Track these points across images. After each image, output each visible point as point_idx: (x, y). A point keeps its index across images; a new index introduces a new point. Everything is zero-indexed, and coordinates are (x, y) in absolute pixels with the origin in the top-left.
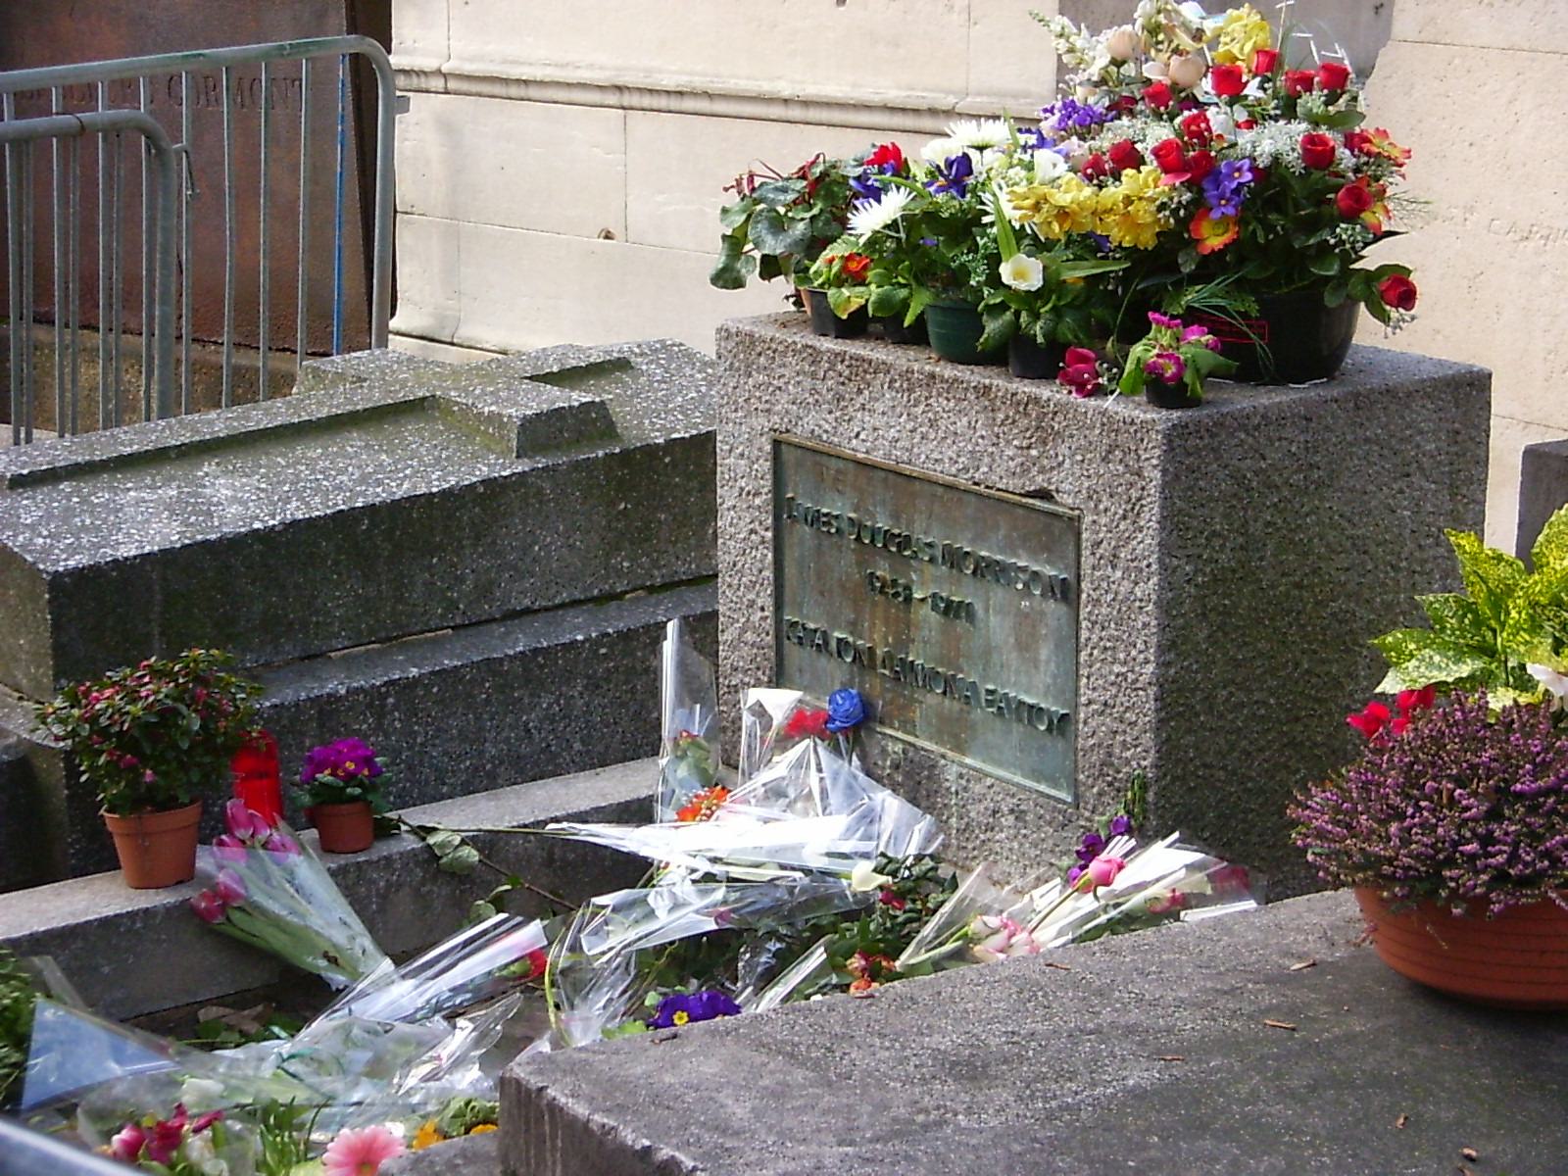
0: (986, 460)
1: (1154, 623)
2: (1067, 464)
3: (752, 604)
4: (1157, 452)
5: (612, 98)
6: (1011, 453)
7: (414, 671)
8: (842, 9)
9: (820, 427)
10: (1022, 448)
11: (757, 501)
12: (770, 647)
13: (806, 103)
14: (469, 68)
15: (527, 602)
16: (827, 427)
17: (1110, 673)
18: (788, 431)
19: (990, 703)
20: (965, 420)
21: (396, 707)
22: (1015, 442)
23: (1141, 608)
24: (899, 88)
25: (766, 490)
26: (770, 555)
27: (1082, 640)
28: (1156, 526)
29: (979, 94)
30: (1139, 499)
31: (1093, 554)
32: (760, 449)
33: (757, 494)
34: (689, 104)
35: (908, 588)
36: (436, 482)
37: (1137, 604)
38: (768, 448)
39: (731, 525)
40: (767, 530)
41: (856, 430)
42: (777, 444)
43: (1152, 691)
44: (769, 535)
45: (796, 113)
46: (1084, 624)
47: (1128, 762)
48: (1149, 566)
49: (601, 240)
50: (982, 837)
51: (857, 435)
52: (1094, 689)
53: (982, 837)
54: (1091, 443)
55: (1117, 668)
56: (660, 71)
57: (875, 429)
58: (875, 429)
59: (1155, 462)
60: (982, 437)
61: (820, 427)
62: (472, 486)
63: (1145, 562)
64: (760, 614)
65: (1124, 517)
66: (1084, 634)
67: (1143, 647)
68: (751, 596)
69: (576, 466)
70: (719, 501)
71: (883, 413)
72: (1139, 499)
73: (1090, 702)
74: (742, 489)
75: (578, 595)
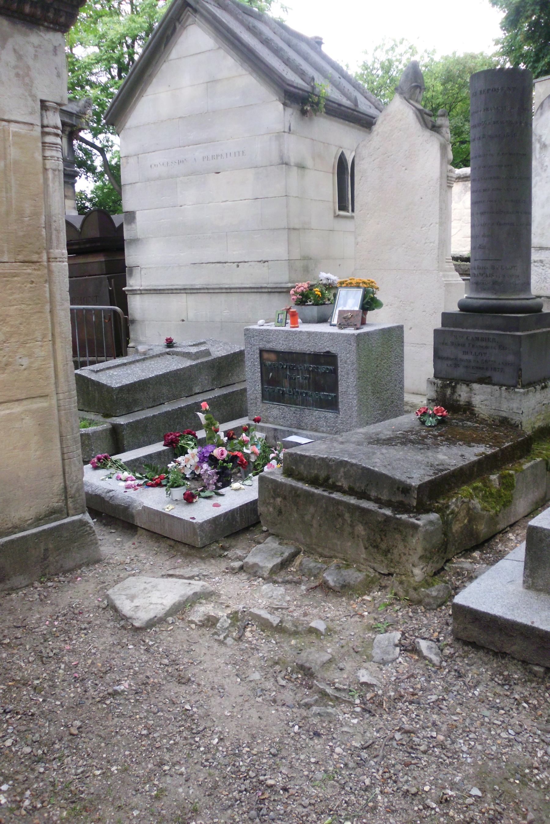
13: (231, 288)
14: (147, 288)
36: (181, 366)
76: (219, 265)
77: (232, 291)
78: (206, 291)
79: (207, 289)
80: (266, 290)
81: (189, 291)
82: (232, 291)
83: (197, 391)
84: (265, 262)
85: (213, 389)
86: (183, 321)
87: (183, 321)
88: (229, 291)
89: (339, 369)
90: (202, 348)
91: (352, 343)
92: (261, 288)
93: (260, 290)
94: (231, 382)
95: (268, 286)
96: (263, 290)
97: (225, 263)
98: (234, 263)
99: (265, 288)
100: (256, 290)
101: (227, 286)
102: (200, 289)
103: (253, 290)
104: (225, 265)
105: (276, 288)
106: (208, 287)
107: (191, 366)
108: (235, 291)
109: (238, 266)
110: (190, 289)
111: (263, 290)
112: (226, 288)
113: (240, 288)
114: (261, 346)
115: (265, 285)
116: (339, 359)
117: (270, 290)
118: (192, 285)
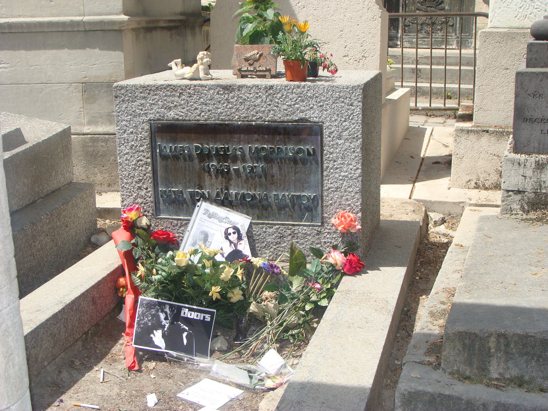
0: (272, 112)
1: (360, 155)
2: (315, 107)
3: (140, 188)
10: (290, 106)
11: (142, 148)
12: (152, 202)
17: (339, 176)
20: (260, 100)
22: (287, 104)
26: (150, 168)
27: (325, 167)
28: (360, 122)
30: (352, 114)
31: (330, 137)
33: (141, 146)
37: (352, 150)
38: (147, 127)
39: (126, 160)
40: (147, 158)
41: (199, 113)
43: (360, 179)
44: (149, 160)
46: (325, 162)
47: (349, 205)
48: (357, 136)
50: (275, 247)
51: (199, 115)
52: (331, 183)
54: (327, 98)
55: (343, 174)
57: (209, 111)
59: (359, 99)
65: (345, 121)
66: (325, 165)
68: (140, 184)
71: (214, 104)
72: (352, 114)
73: (329, 188)
74: (133, 145)
91: (356, 103)
114: (151, 116)
116: (326, 132)
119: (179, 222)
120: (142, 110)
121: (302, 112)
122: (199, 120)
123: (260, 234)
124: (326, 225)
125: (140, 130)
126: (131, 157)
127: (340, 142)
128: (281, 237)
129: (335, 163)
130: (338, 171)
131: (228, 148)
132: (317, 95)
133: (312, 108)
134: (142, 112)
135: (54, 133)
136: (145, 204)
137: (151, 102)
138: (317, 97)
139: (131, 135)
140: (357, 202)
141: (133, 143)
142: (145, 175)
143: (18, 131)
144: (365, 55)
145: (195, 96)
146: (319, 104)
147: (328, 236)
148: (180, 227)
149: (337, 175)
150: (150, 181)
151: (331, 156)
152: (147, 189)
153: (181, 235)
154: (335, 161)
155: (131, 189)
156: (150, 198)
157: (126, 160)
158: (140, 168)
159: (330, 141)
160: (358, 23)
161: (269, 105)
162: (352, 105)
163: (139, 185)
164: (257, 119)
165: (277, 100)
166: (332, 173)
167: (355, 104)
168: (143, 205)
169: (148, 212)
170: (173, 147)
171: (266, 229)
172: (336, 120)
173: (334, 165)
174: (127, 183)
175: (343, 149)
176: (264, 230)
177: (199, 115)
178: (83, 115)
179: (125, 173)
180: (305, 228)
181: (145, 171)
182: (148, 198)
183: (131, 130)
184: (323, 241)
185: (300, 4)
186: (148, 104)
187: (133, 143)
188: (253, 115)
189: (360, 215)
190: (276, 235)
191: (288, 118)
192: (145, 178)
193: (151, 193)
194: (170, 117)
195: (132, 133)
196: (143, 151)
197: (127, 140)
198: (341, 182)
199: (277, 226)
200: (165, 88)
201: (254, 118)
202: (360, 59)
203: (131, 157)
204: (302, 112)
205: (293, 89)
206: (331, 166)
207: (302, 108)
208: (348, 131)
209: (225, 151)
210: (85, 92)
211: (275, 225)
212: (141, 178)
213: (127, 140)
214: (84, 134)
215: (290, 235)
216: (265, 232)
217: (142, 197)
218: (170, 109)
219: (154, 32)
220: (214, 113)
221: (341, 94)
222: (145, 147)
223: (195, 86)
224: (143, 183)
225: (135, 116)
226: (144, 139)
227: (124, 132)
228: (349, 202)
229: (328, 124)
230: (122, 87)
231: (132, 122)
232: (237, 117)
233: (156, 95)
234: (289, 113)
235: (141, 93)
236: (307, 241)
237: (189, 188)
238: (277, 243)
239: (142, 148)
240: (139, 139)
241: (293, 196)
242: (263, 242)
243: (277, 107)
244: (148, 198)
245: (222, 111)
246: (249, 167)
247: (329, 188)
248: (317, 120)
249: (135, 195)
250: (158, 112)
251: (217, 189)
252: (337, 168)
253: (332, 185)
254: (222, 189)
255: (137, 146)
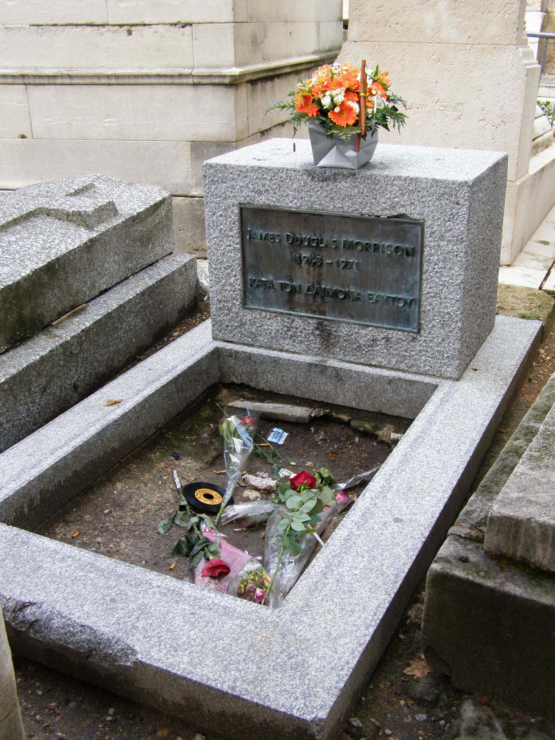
4: (468, 194)
5: (20, 81)
6: (384, 201)
7: (88, 324)
8: (131, 37)
9: (268, 200)
11: (231, 233)
15: (105, 287)
16: (274, 200)
18: (248, 203)
19: (370, 299)
20: (356, 190)
21: (85, 341)
22: (386, 197)
23: (457, 255)
24: (161, 67)
25: (236, 228)
26: (239, 255)
27: (424, 270)
29: (199, 67)
30: (457, 214)
31: (431, 237)
32: (232, 212)
33: (231, 230)
34: (59, 81)
35: (322, 259)
37: (455, 253)
38: (237, 211)
39: (215, 245)
42: (241, 210)
44: (239, 246)
45: (113, 81)
46: (425, 264)
47: (448, 313)
49: (20, 139)
52: (430, 288)
53: (366, 350)
55: (443, 279)
56: (42, 68)
58: (302, 198)
59: (466, 198)
60: (367, 196)
61: (269, 200)
62: (86, 244)
63: (460, 237)
64: (233, 279)
65: (449, 221)
66: (425, 267)
67: (458, 269)
69: (115, 228)
70: (207, 235)
72: (457, 214)
73: (428, 293)
74: (222, 229)
75: (119, 280)
76: (89, 29)
77: (120, 81)
78: (67, 81)
79: (70, 76)
80: (190, 81)
81: (31, 81)
82: (120, 81)
83: (104, 287)
84: (184, 26)
85: (127, 278)
86: (23, 137)
87: (23, 137)
88: (113, 81)
89: (427, 250)
90: (103, 201)
91: (461, 201)
92: (181, 76)
93: (177, 81)
94: (153, 259)
95: (195, 72)
96: (184, 81)
97: (103, 25)
98: (121, 26)
99: (190, 76)
100: (168, 81)
101: (109, 72)
102: (55, 77)
103: (162, 81)
104: (102, 29)
105: (210, 76)
106: (70, 73)
107: (91, 240)
108: (127, 81)
109: (130, 33)
110: (34, 76)
111: (184, 81)
112: (108, 77)
113: (136, 76)
115: (187, 71)
116: (427, 231)
117: (196, 81)
118: (36, 68)
119: (268, 314)
120: (231, 192)
121: (403, 206)
122: (291, 208)
123: (352, 335)
124: (422, 332)
125: (230, 214)
126: (220, 241)
127: (442, 244)
128: (373, 340)
129: (436, 266)
130: (438, 275)
131: (321, 239)
132: (419, 189)
133: (412, 203)
134: (232, 195)
135: (152, 203)
136: (233, 292)
137: (241, 184)
138: (419, 192)
139: (220, 218)
140: (457, 311)
141: (222, 227)
142: (234, 261)
143: (111, 204)
144: (505, 120)
145: (287, 181)
146: (421, 200)
147: (424, 344)
148: (269, 319)
149: (437, 280)
150: (239, 269)
151: (432, 258)
152: (235, 276)
153: (270, 328)
154: (435, 264)
155: (219, 275)
156: (239, 285)
157: (215, 245)
158: (229, 254)
159: (431, 242)
160: (499, 82)
161: (367, 196)
162: (457, 203)
163: (227, 272)
164: (352, 211)
165: (375, 192)
166: (432, 277)
167: (460, 203)
168: (232, 293)
169: (237, 301)
170: (264, 234)
171: (359, 330)
172: (438, 219)
173: (434, 268)
174: (215, 269)
175: (446, 252)
176: (356, 331)
177: (291, 202)
178: (190, 176)
179: (214, 258)
180: (400, 333)
181: (234, 257)
182: (236, 286)
183: (221, 213)
184: (418, 348)
185: (434, 56)
186: (238, 187)
187: (222, 227)
188: (348, 206)
189: (459, 324)
190: (368, 337)
191: (387, 212)
192: (234, 264)
193: (239, 280)
194: (261, 202)
195: (221, 216)
196: (232, 236)
197: (216, 223)
198: (441, 288)
199: (370, 328)
200: (256, 170)
201: (350, 210)
202: (498, 125)
203: (220, 241)
204: (403, 206)
205: (394, 181)
206: (430, 269)
207: (402, 203)
208: (452, 232)
209: (317, 243)
210: (193, 151)
211: (368, 326)
212: (230, 265)
213: (216, 223)
214: (191, 197)
215: (383, 338)
216: (357, 333)
217: (231, 285)
218: (260, 193)
219: (276, 80)
220: (308, 201)
221: (447, 190)
222: (235, 231)
223: (287, 170)
224: (232, 270)
225: (225, 199)
226: (234, 224)
227: (213, 215)
228: (449, 310)
229: (430, 222)
230: (211, 166)
231: (221, 205)
232: (331, 207)
233: (246, 177)
234: (388, 207)
235: (231, 173)
236: (401, 347)
237: (279, 279)
238: (369, 346)
239: (231, 233)
240: (228, 223)
241: (388, 297)
242: (355, 344)
243: (375, 199)
244: (236, 286)
245: (316, 199)
246: (343, 262)
247: (428, 293)
248: (418, 217)
249: (224, 281)
250: (248, 196)
251: (309, 283)
252: (437, 272)
253: (431, 290)
254: (313, 284)
255: (226, 230)
